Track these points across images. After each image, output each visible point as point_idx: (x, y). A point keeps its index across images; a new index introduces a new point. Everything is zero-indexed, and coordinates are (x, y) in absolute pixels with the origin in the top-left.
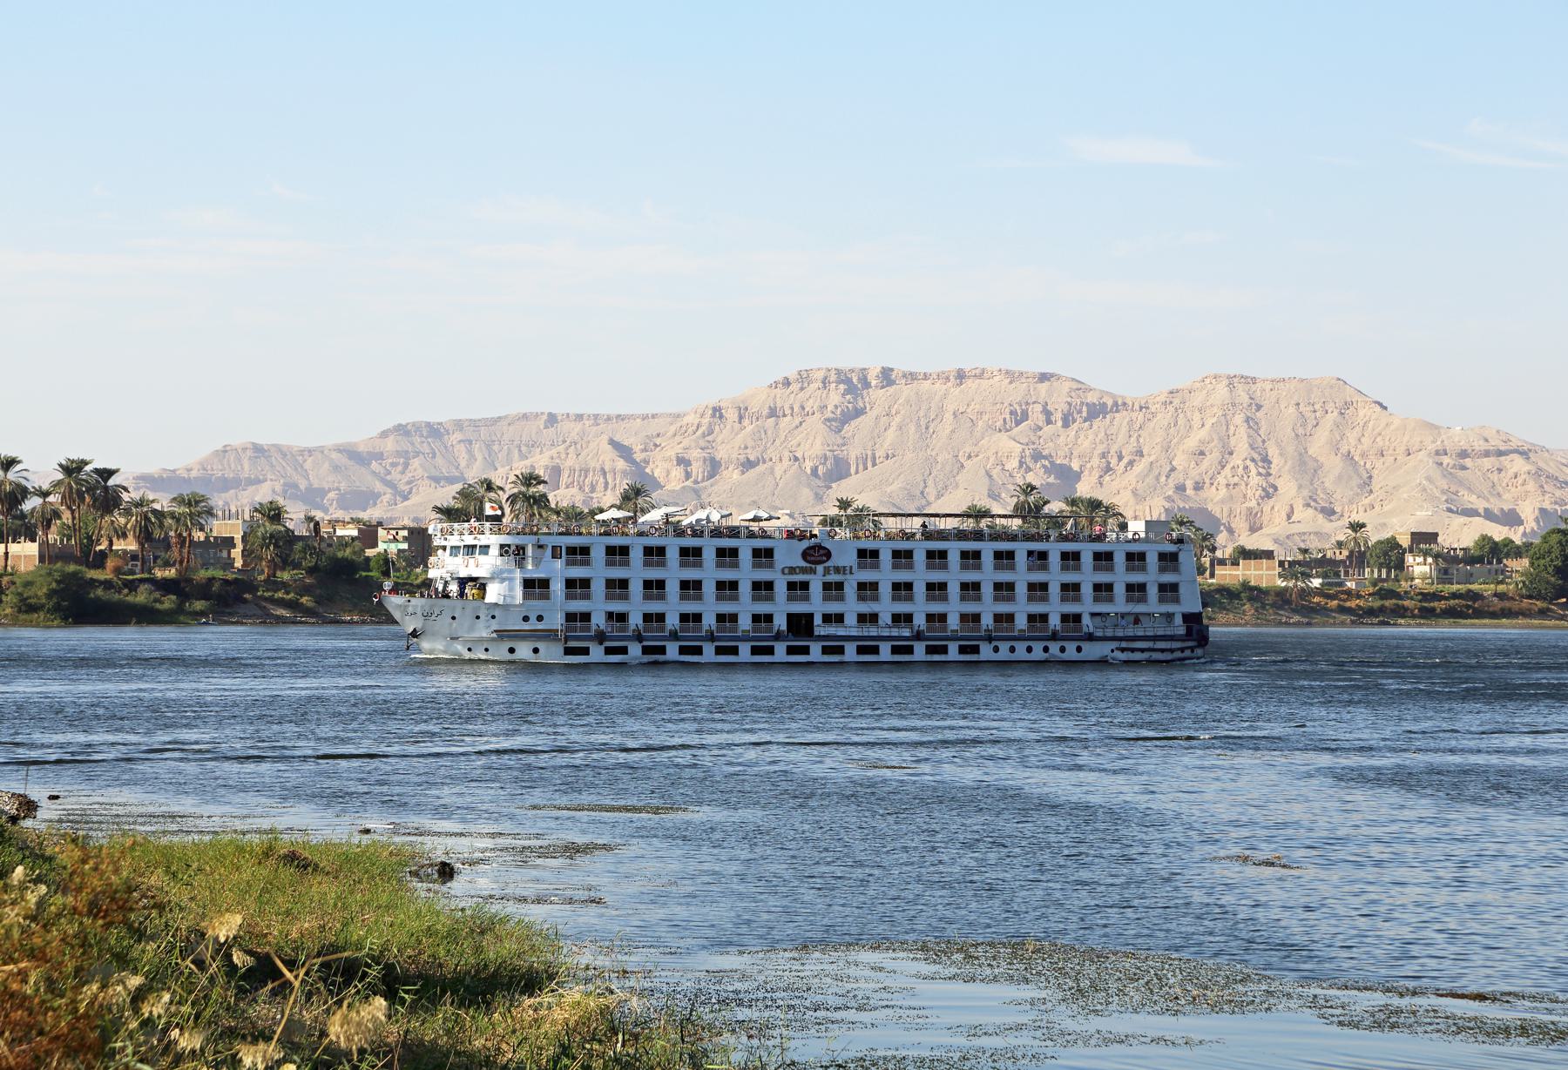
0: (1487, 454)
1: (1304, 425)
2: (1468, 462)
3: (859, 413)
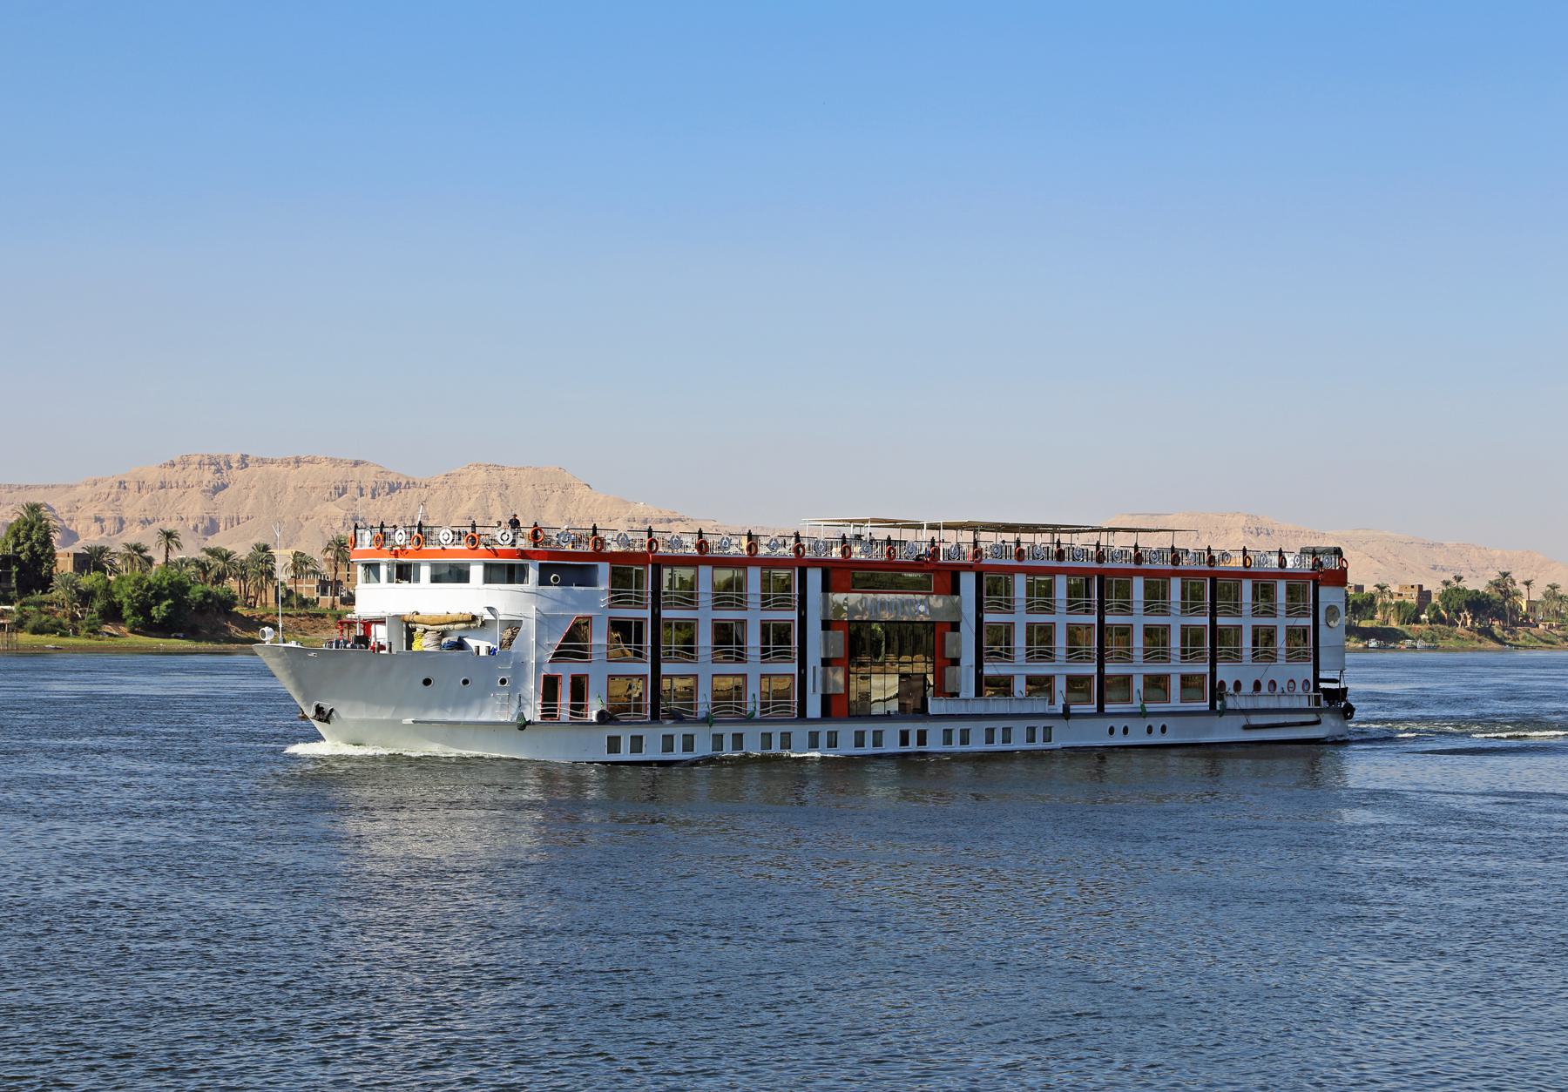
3: (225, 486)
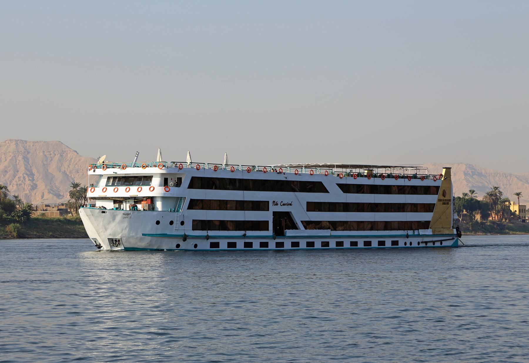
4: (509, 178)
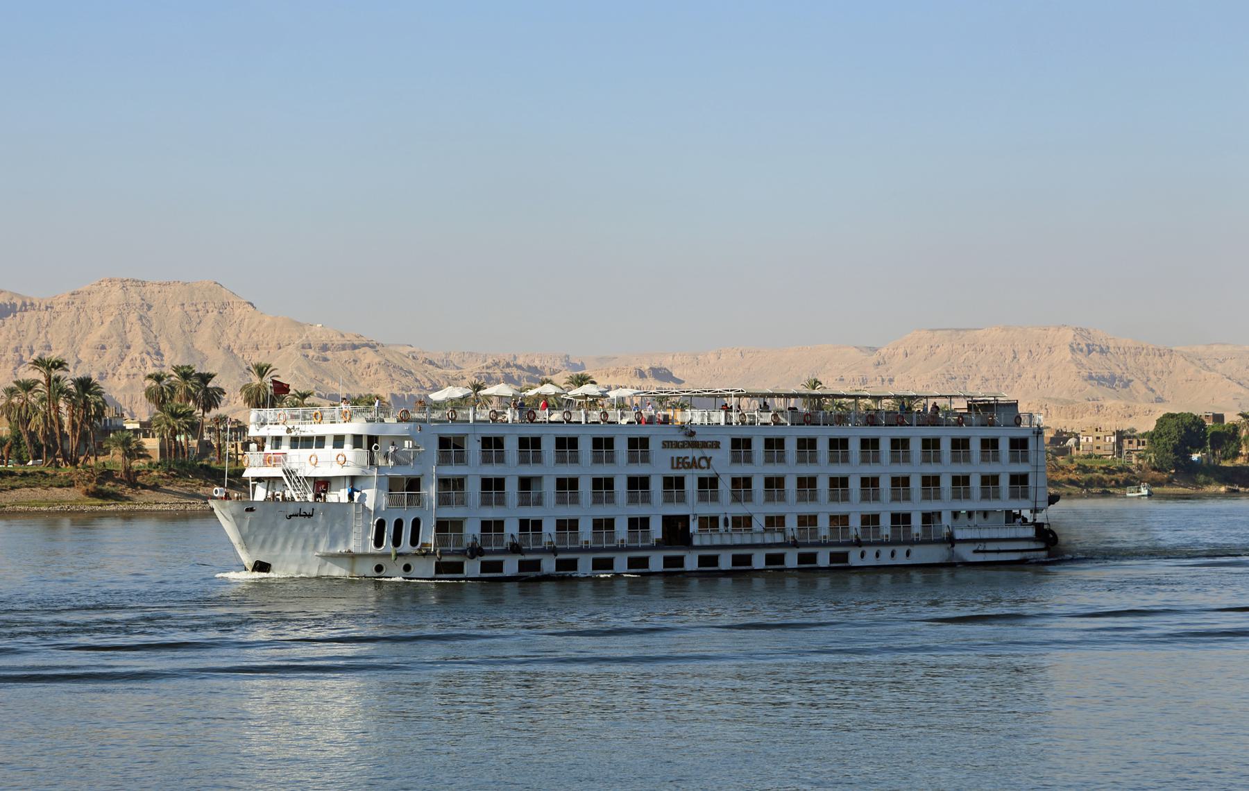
0: (344, 348)
1: (189, 323)
2: (329, 354)
4: (1167, 357)
